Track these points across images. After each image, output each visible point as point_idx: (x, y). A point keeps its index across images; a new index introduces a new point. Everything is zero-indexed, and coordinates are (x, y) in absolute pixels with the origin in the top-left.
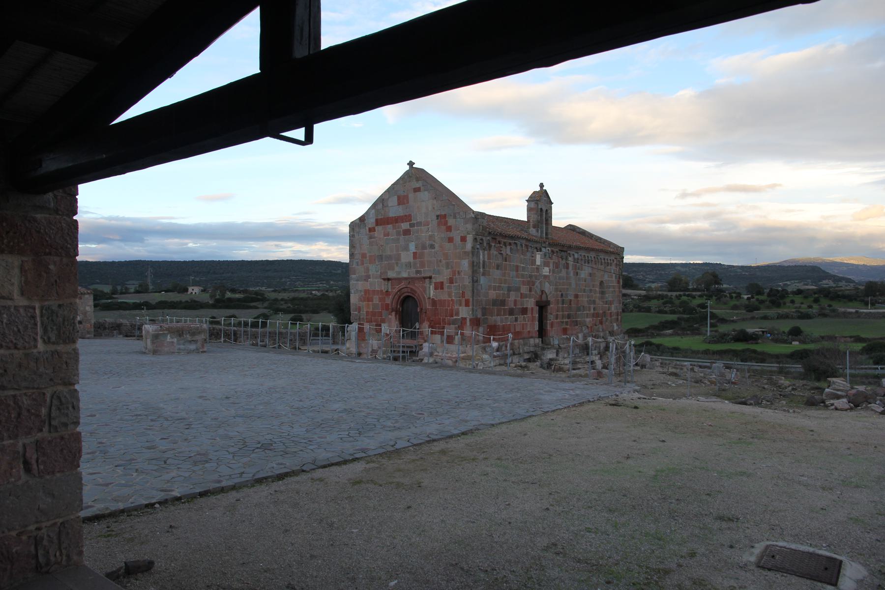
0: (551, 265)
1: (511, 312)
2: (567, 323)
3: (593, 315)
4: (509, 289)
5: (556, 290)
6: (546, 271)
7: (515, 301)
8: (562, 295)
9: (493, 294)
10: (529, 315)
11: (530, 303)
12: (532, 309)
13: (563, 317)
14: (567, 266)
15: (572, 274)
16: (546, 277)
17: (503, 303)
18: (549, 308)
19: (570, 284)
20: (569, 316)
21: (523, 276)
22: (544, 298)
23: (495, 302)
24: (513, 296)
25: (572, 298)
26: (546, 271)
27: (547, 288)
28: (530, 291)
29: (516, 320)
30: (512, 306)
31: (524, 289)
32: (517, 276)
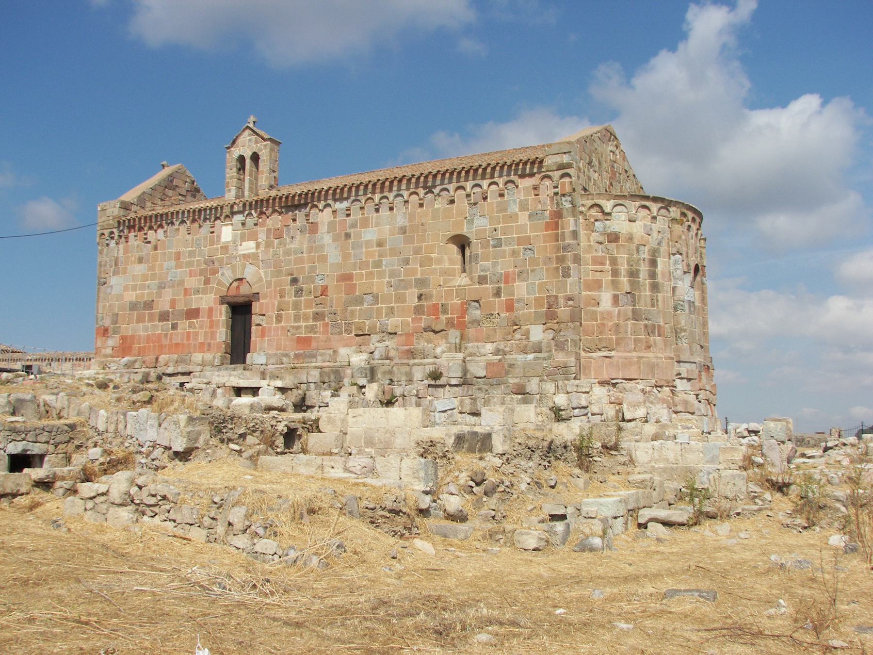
0: (262, 237)
1: (164, 317)
2: (312, 329)
3: (418, 310)
4: (161, 287)
5: (278, 273)
6: (248, 247)
7: (173, 302)
8: (295, 281)
9: (131, 296)
10: (204, 319)
11: (207, 301)
12: (211, 310)
13: (297, 318)
14: (313, 228)
15: (327, 239)
16: (246, 257)
17: (149, 305)
18: (256, 308)
19: (323, 259)
20: (318, 316)
21: (190, 264)
22: (245, 290)
23: (133, 306)
24: (168, 295)
25: (332, 283)
26: (248, 247)
27: (249, 272)
28: (207, 282)
29: (174, 327)
30: (167, 308)
31: (193, 282)
32: (178, 266)
